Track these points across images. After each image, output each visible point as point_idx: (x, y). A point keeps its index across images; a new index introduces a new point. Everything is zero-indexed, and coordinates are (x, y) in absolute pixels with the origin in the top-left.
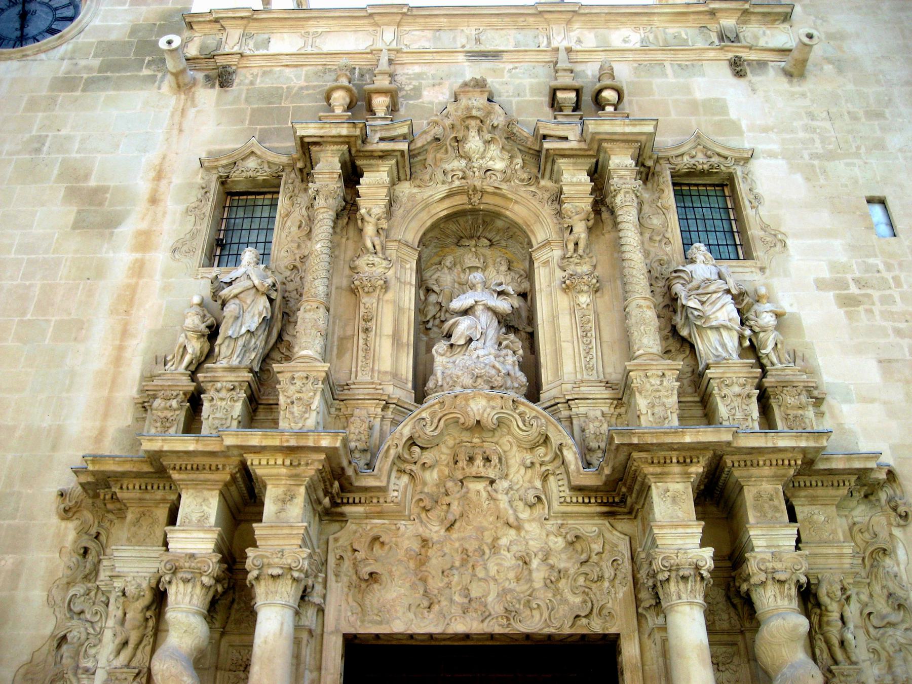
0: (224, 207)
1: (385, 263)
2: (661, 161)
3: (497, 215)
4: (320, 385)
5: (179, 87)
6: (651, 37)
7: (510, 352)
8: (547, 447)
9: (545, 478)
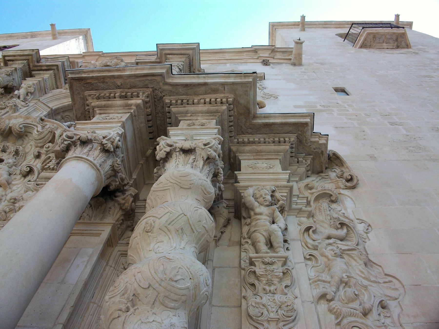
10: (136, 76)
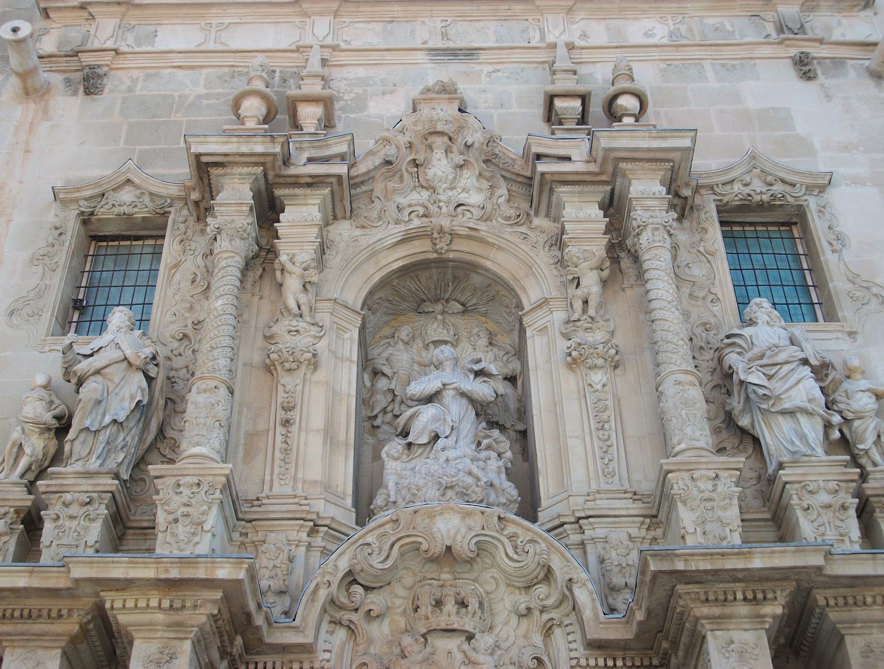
0: (86, 256)
1: (314, 330)
2: (703, 191)
3: (471, 267)
4: (218, 494)
5: (27, 93)
6: (683, 29)
7: (493, 454)
8: (549, 585)
9: (548, 631)
10: (773, 569)
